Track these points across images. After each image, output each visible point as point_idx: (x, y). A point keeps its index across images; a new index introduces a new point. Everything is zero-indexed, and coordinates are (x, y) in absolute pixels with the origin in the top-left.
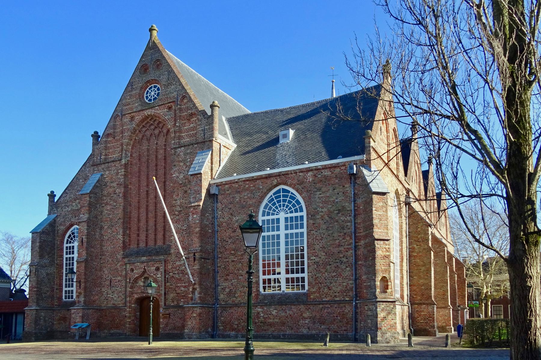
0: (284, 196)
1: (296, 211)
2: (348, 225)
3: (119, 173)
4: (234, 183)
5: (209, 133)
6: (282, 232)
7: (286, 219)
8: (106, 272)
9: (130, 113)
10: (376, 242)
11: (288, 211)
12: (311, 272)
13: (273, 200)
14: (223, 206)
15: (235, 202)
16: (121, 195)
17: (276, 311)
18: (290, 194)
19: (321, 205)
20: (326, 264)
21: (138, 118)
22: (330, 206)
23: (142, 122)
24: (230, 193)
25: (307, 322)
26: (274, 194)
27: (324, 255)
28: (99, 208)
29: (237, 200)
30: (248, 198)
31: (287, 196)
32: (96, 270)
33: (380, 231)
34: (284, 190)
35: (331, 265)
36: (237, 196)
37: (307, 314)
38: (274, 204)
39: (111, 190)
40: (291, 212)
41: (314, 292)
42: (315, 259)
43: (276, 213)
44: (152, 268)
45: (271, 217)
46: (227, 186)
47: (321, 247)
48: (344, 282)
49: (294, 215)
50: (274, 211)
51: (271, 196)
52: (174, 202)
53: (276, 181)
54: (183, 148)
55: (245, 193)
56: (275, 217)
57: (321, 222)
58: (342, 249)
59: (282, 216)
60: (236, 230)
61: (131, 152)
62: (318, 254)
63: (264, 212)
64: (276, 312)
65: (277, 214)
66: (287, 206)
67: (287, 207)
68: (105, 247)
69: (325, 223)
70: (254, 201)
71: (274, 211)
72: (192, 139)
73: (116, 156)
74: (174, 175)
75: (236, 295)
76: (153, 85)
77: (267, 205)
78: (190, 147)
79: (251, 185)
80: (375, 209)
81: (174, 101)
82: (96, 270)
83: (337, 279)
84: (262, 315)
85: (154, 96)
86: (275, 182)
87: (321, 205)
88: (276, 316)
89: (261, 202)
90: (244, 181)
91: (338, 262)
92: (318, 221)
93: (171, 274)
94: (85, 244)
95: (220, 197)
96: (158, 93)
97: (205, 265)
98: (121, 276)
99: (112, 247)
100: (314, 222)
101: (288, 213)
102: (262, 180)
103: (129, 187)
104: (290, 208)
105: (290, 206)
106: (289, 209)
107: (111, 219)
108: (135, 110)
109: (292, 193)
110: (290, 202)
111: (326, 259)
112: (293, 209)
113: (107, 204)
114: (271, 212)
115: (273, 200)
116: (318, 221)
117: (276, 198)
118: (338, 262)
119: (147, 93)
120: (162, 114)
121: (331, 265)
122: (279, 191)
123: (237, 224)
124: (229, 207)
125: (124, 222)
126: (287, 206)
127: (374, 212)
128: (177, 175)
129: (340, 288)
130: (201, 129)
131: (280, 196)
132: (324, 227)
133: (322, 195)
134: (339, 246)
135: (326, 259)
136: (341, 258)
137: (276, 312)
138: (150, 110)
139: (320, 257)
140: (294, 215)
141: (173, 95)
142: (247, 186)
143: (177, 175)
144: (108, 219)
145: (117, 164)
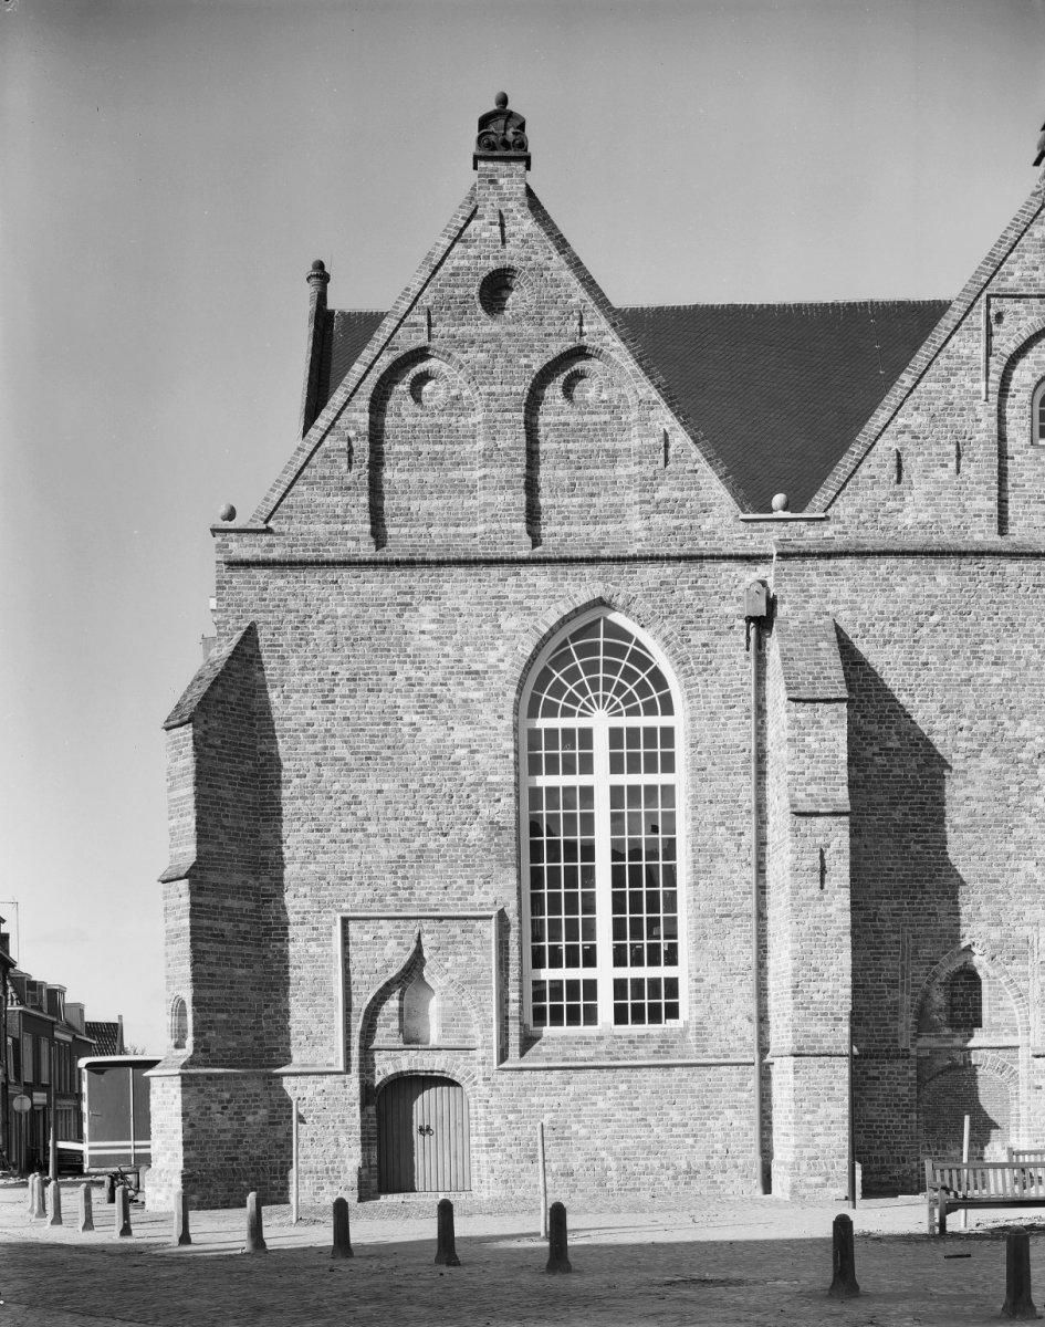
1: (650, 710)
7: (615, 735)
13: (567, 657)
18: (631, 646)
31: (620, 651)
40: (633, 712)
49: (642, 721)
51: (565, 643)
56: (575, 723)
59: (600, 722)
65: (581, 715)
101: (620, 714)
104: (629, 699)
109: (638, 643)
117: (582, 651)
131: (593, 649)
140: (642, 721)
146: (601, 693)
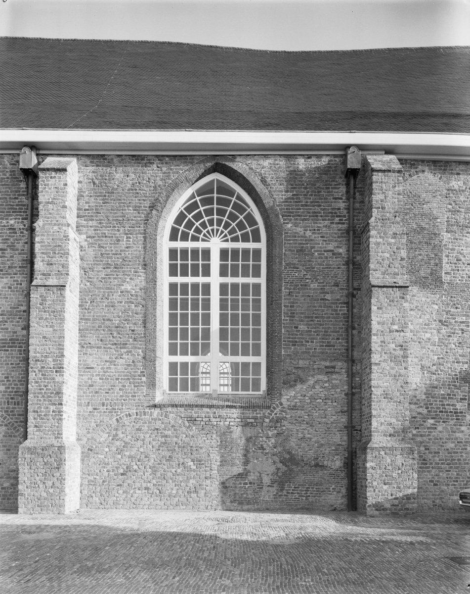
0: (220, 201)
1: (245, 238)
7: (224, 253)
31: (227, 203)
34: (223, 189)
45: (190, 245)
49: (241, 245)
50: (198, 231)
56: (200, 245)
65: (203, 240)
71: (198, 231)
101: (227, 241)
109: (239, 198)
117: (205, 202)
140: (241, 245)
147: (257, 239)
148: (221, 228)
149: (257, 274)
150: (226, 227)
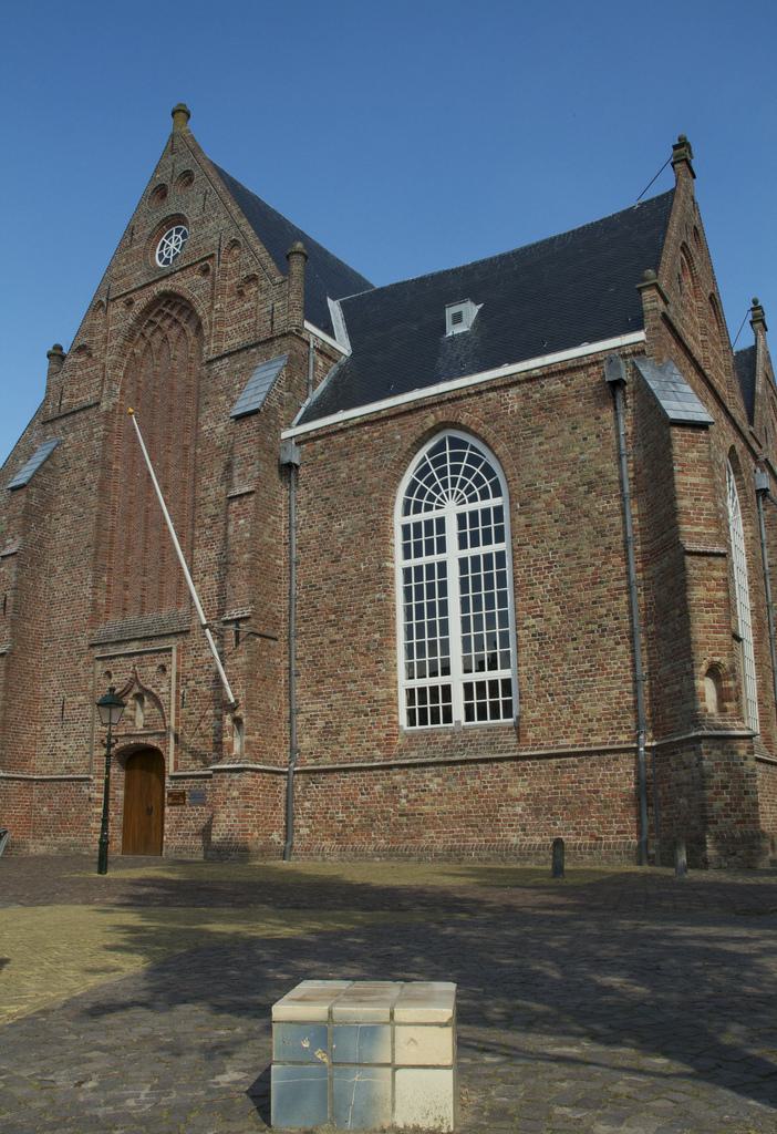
0: (455, 457)
2: (614, 525)
3: (93, 434)
4: (335, 433)
5: (282, 318)
6: (453, 555)
7: (461, 517)
8: (55, 683)
9: (125, 294)
10: (689, 559)
11: (466, 497)
12: (526, 664)
13: (427, 469)
14: (311, 495)
15: (339, 480)
16: (95, 487)
17: (439, 780)
19: (545, 474)
20: (561, 639)
21: (141, 302)
22: (569, 474)
23: (148, 313)
24: (327, 460)
25: (519, 810)
26: (430, 454)
27: (558, 614)
28: (50, 522)
29: (343, 475)
30: (369, 468)
31: (459, 457)
32: (34, 678)
33: (697, 529)
34: (455, 443)
35: (575, 639)
36: (343, 465)
37: (519, 788)
38: (430, 481)
39: (76, 477)
40: (473, 499)
41: (536, 722)
42: (534, 626)
43: (435, 504)
44: (150, 669)
45: (423, 517)
46: (319, 442)
47: (548, 591)
48: (613, 689)
49: (480, 505)
50: (431, 498)
51: (424, 460)
52: (202, 494)
53: (432, 417)
54: (226, 360)
55: (360, 456)
56: (434, 515)
57: (547, 519)
58: (603, 591)
59: (450, 510)
60: (340, 556)
61: (123, 384)
62: (542, 611)
63: (407, 504)
64: (438, 785)
65: (437, 508)
66: (463, 483)
67: (461, 487)
68: (56, 620)
69: (556, 521)
70: (382, 474)
72: (246, 336)
73: (88, 399)
74: (205, 428)
75: (342, 738)
76: (174, 229)
77: (413, 484)
78: (241, 355)
79: (375, 434)
80: (680, 468)
81: (212, 256)
82: (34, 678)
83: (594, 681)
84: (404, 792)
85: (174, 251)
86: (431, 421)
87: (545, 474)
88: (440, 795)
89: (399, 479)
90: (359, 425)
91: (593, 632)
92: (538, 518)
93: (191, 683)
94: (10, 611)
95: (302, 471)
96: (183, 243)
97: (264, 653)
98: (84, 692)
99: (70, 617)
100: (527, 522)
101: (464, 503)
102: (401, 420)
103: (114, 467)
104: (470, 489)
105: (470, 481)
106: (461, 487)
107: (72, 548)
108: (134, 286)
109: (473, 448)
110: (468, 473)
111: (563, 622)
112: (477, 490)
113: (65, 512)
114: (424, 501)
115: (427, 469)
116: (538, 518)
118: (593, 632)
119: (161, 249)
120: (186, 287)
121: (575, 639)
122: (440, 447)
123: (341, 540)
124: (325, 496)
125: (96, 554)
126: (463, 483)
127: (678, 478)
128: (213, 425)
129: (602, 705)
130: (266, 310)
132: (554, 532)
133: (546, 447)
134: (594, 584)
135: (563, 622)
136: (601, 617)
137: (438, 785)
138: (164, 282)
139: (549, 619)
140: (480, 505)
141: (211, 241)
142: (366, 437)
143: (213, 425)
144: (66, 549)
145: (91, 414)
146: (456, 489)
147: (497, 493)
148: (450, 488)
149: (500, 539)
150: (445, 487)
